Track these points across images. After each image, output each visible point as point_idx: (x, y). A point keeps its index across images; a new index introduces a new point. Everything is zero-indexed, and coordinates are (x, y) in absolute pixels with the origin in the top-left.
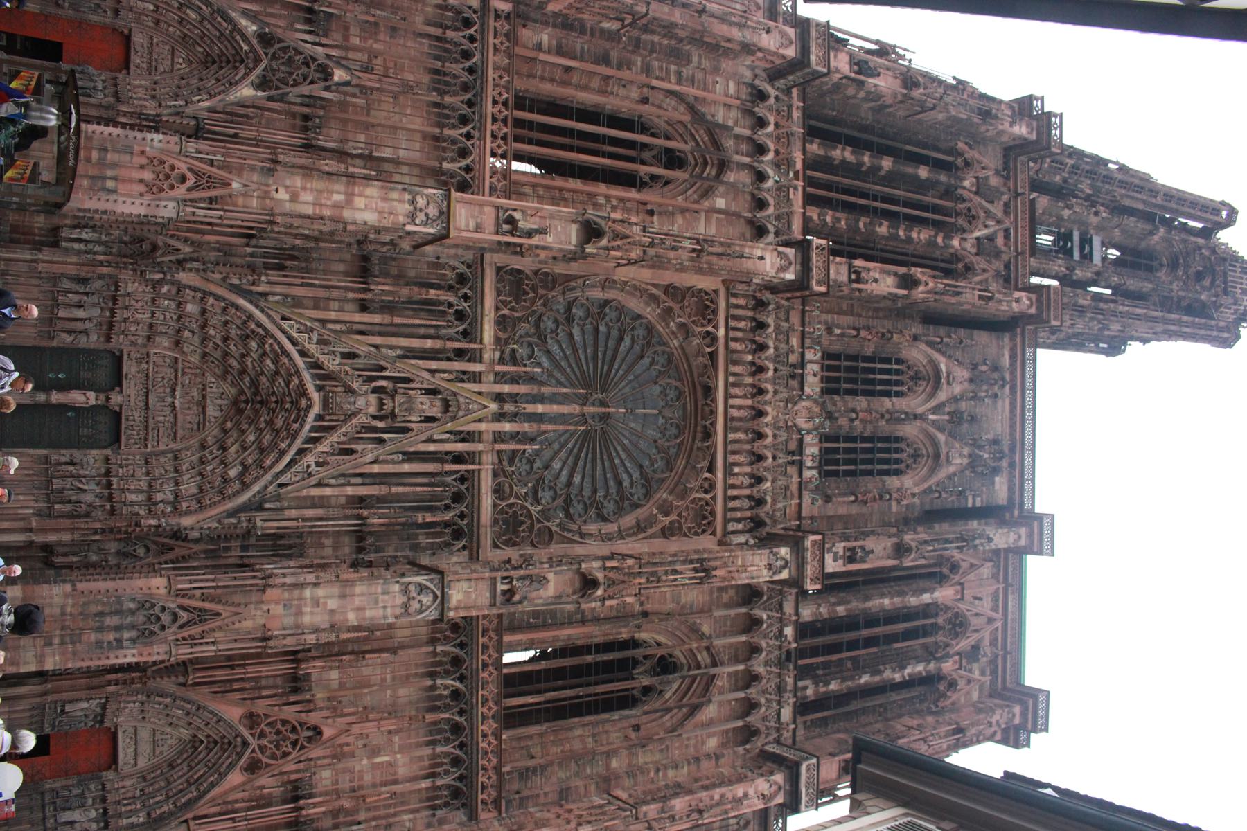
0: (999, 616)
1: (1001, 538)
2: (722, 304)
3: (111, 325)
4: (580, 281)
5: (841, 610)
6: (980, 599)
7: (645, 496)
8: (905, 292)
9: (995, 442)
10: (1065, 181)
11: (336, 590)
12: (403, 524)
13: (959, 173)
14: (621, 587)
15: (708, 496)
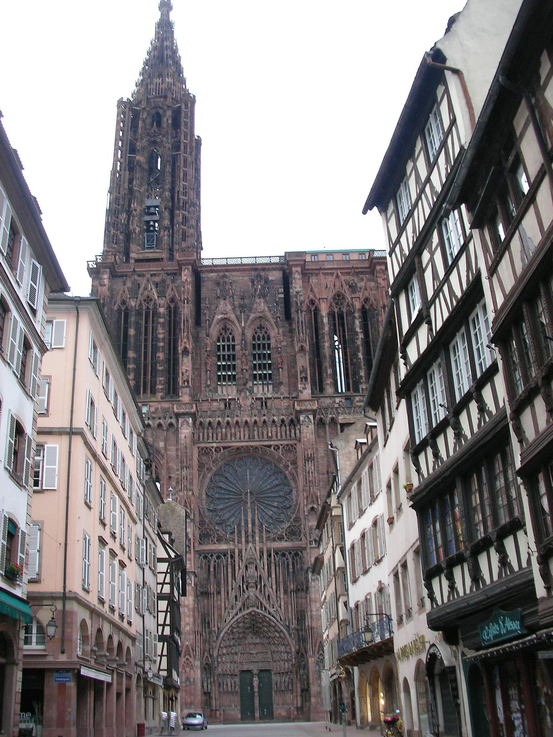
0: (335, 272)
1: (297, 286)
2: (203, 445)
3: (232, 675)
4: (200, 509)
5: (329, 371)
6: (327, 286)
7: (281, 473)
8: (190, 355)
9: (253, 282)
10: (122, 233)
11: (313, 605)
12: (293, 576)
13: (129, 308)
14: (314, 496)
15: (281, 447)
